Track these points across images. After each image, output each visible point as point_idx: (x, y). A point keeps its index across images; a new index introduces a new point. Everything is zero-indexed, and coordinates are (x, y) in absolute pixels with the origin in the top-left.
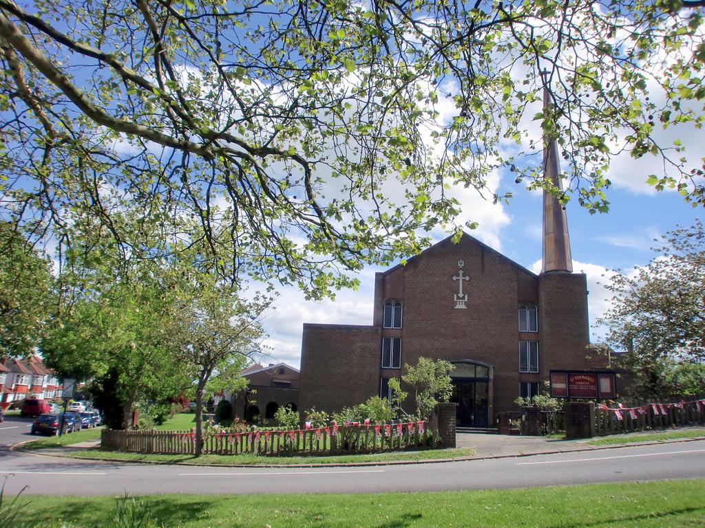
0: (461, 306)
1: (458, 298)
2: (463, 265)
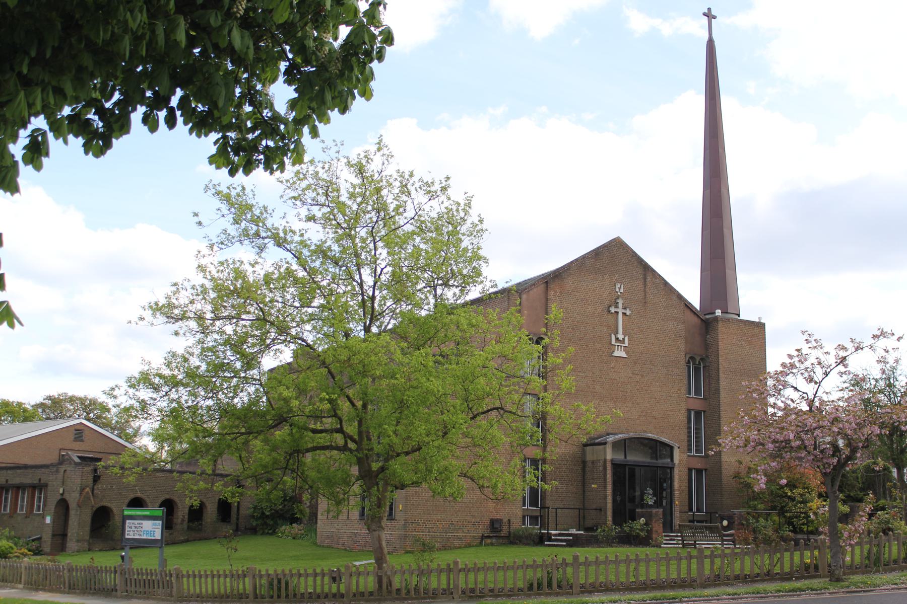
0: (620, 353)
1: (617, 339)
2: (622, 291)
